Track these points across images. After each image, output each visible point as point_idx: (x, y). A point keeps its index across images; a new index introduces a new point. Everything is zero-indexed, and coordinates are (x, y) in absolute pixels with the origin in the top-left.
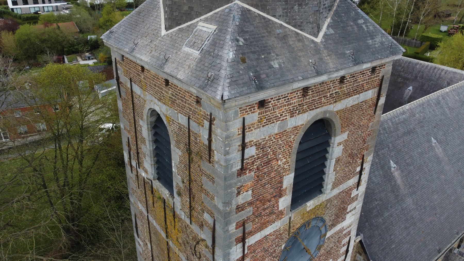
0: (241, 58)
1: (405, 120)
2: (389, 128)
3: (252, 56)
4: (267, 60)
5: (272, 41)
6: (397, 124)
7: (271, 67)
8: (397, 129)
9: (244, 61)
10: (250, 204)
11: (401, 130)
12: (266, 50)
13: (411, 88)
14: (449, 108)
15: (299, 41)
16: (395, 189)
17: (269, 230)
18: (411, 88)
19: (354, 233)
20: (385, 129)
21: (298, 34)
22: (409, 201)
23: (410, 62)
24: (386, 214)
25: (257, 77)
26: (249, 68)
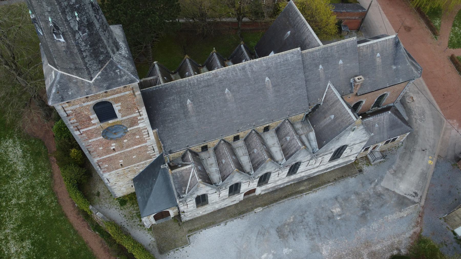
0: (58, 92)
1: (208, 79)
2: (194, 83)
3: (62, 91)
4: (67, 92)
5: (71, 85)
6: (201, 81)
7: (68, 94)
8: (200, 84)
9: (58, 93)
10: (77, 122)
11: (203, 84)
12: (68, 88)
13: (289, 32)
14: (252, 72)
15: (83, 83)
16: (186, 113)
17: (90, 128)
18: (289, 32)
19: (150, 128)
20: (190, 84)
21: (83, 81)
22: (194, 119)
23: (297, 12)
24: (175, 123)
25: (62, 98)
26: (60, 95)
